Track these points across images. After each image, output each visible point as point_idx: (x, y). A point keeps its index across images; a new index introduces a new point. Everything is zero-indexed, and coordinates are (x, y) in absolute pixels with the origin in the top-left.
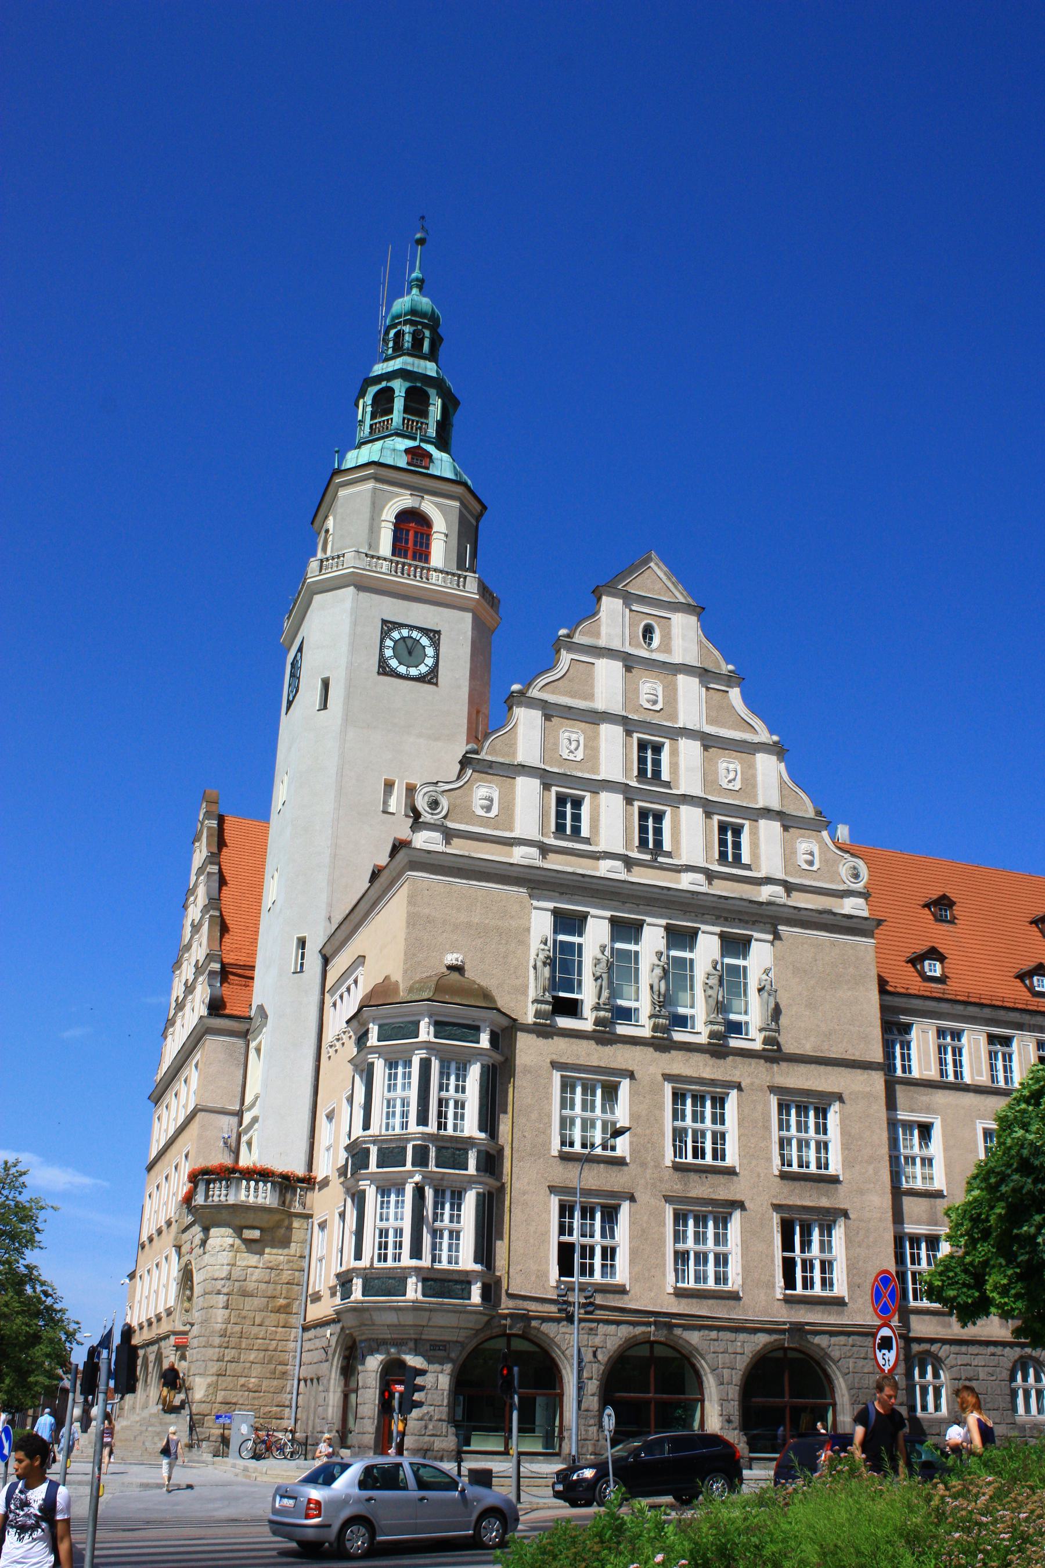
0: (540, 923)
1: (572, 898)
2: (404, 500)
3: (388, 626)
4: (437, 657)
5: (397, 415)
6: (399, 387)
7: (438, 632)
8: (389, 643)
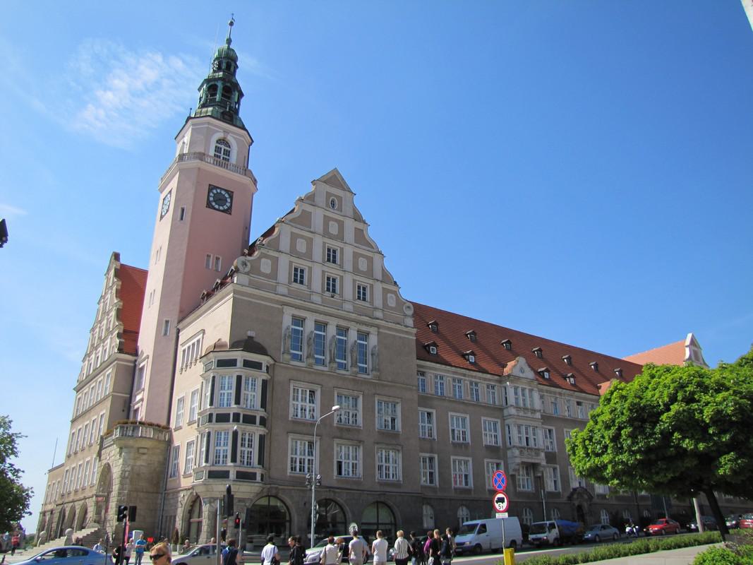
2: (220, 135)
4: (231, 203)
5: (218, 97)
6: (220, 85)
8: (211, 194)
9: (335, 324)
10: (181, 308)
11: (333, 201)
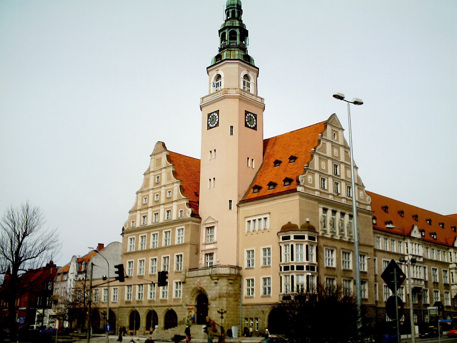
2: (244, 72)
3: (247, 112)
7: (256, 115)
9: (340, 211)
10: (238, 193)
11: (335, 134)
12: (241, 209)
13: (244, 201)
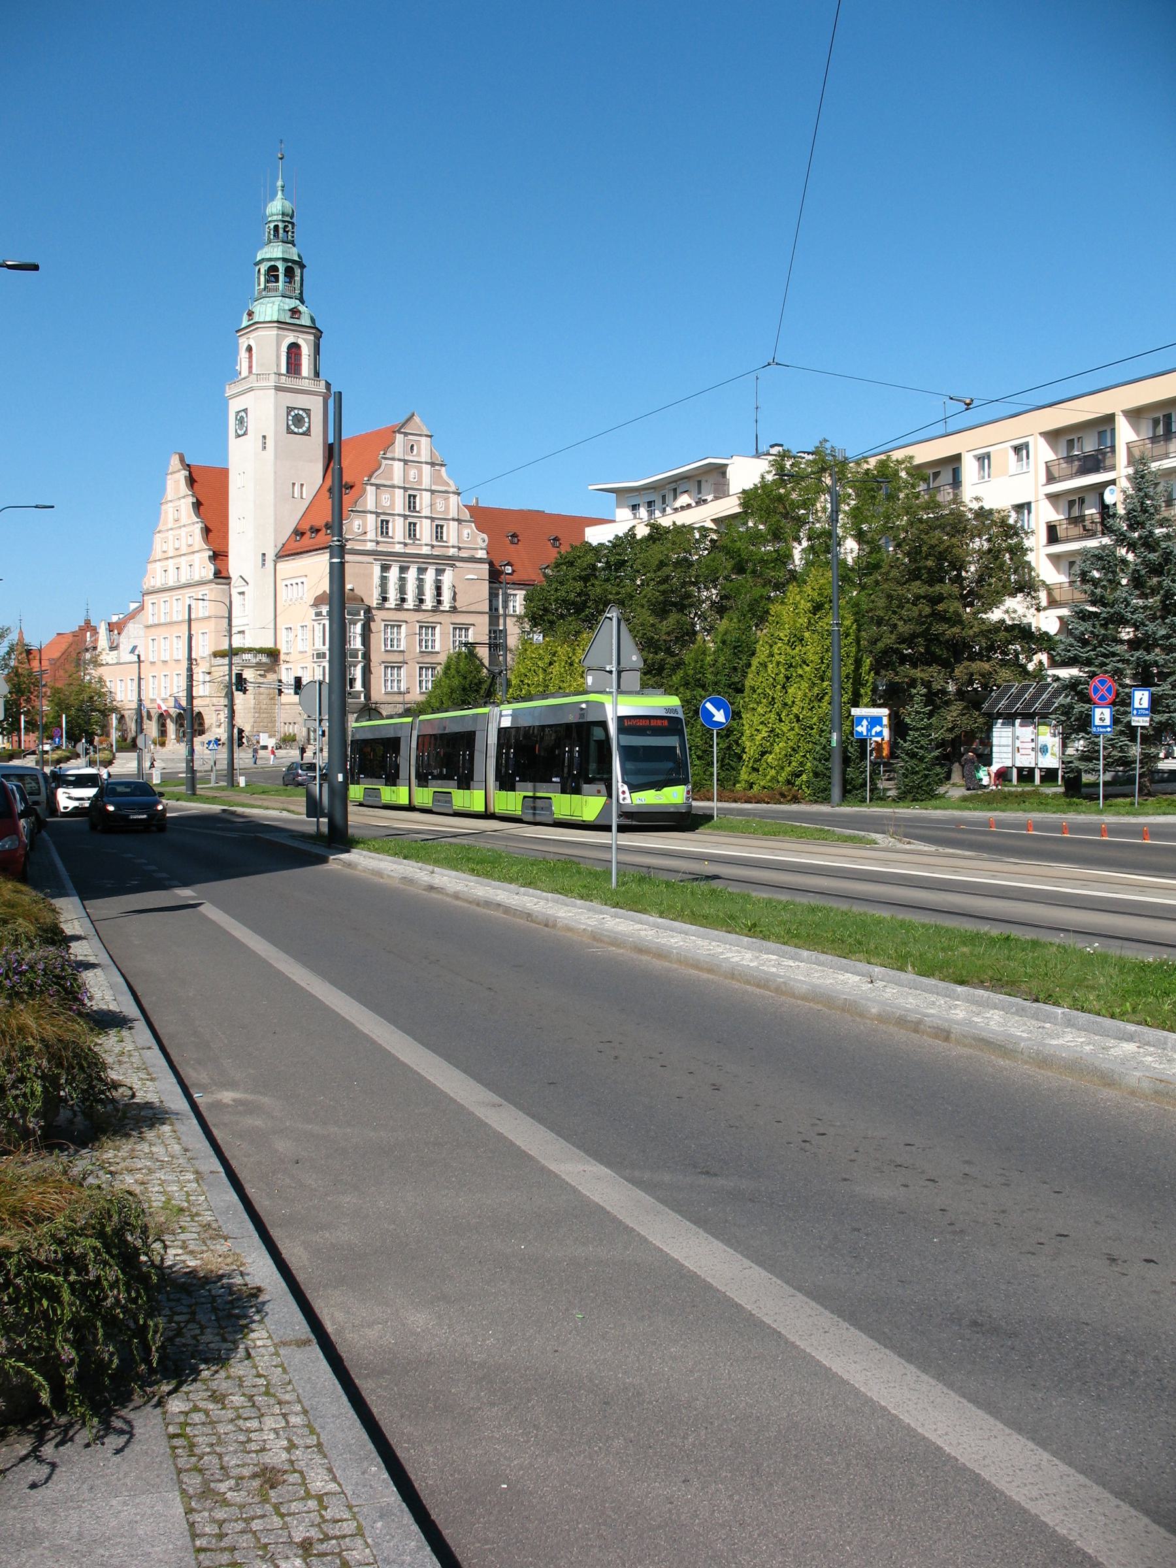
0: (377, 570)
1: (385, 560)
2: (290, 338)
3: (290, 409)
6: (281, 266)
12: (280, 566)
13: (284, 554)
